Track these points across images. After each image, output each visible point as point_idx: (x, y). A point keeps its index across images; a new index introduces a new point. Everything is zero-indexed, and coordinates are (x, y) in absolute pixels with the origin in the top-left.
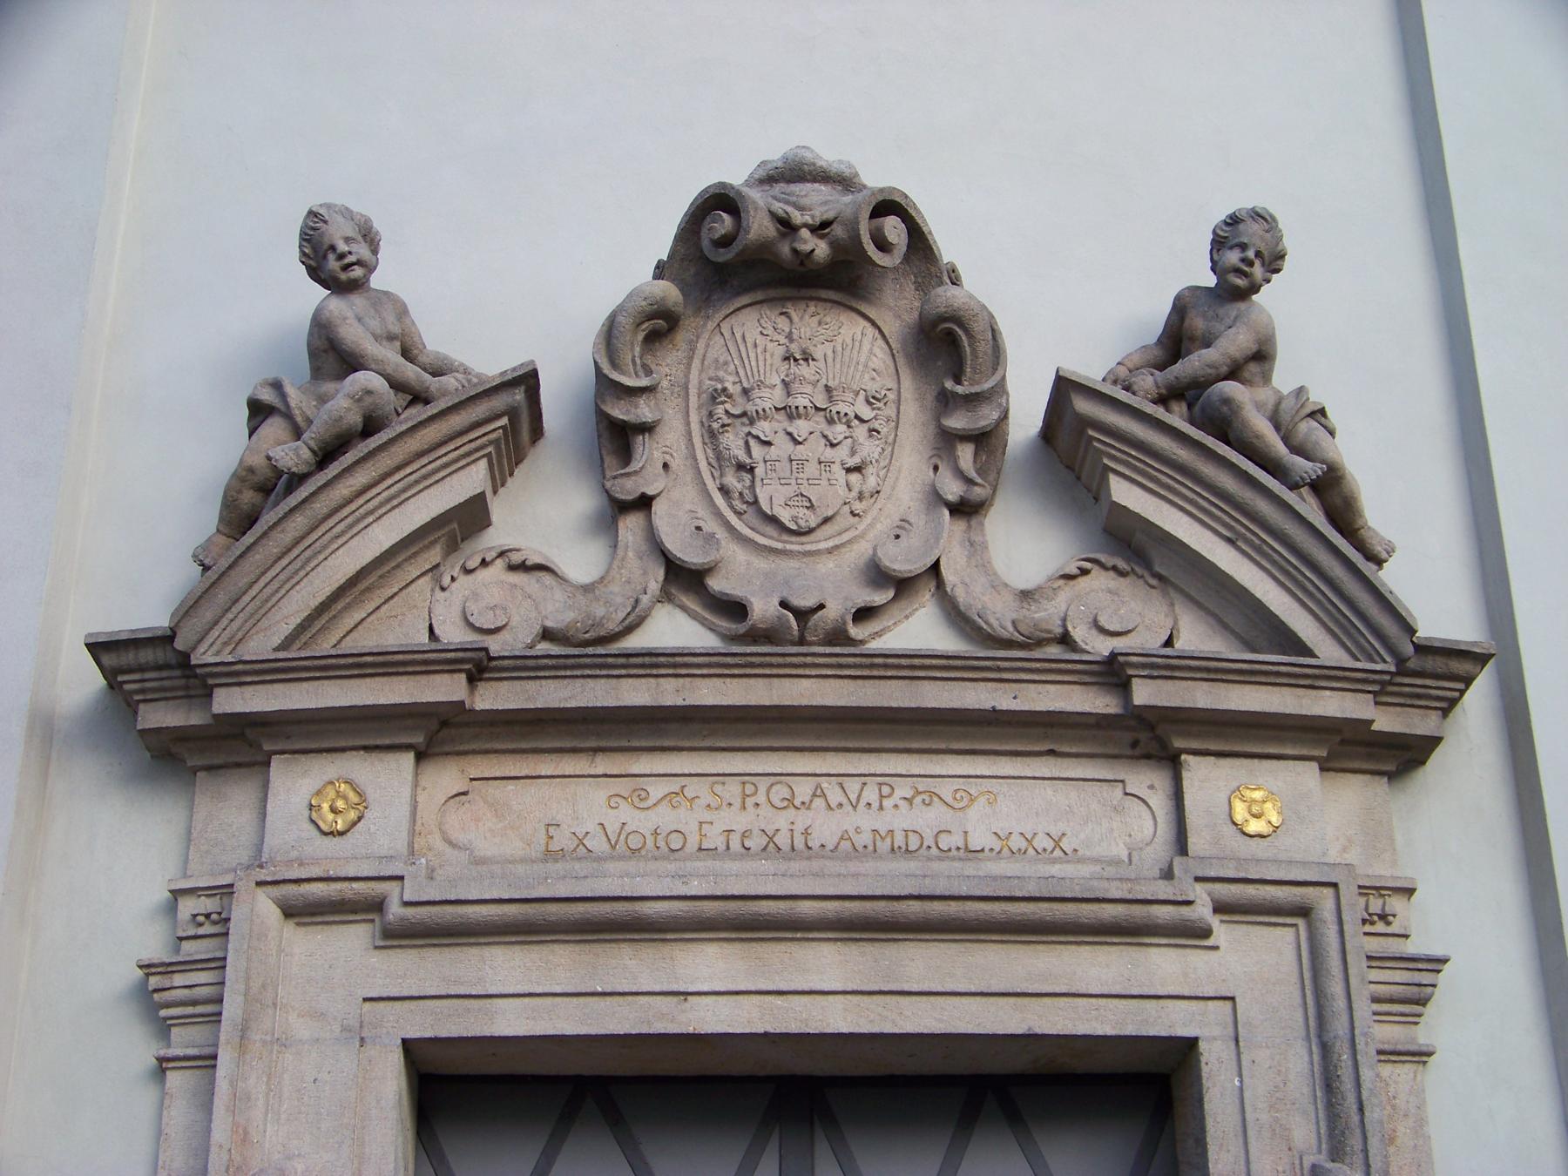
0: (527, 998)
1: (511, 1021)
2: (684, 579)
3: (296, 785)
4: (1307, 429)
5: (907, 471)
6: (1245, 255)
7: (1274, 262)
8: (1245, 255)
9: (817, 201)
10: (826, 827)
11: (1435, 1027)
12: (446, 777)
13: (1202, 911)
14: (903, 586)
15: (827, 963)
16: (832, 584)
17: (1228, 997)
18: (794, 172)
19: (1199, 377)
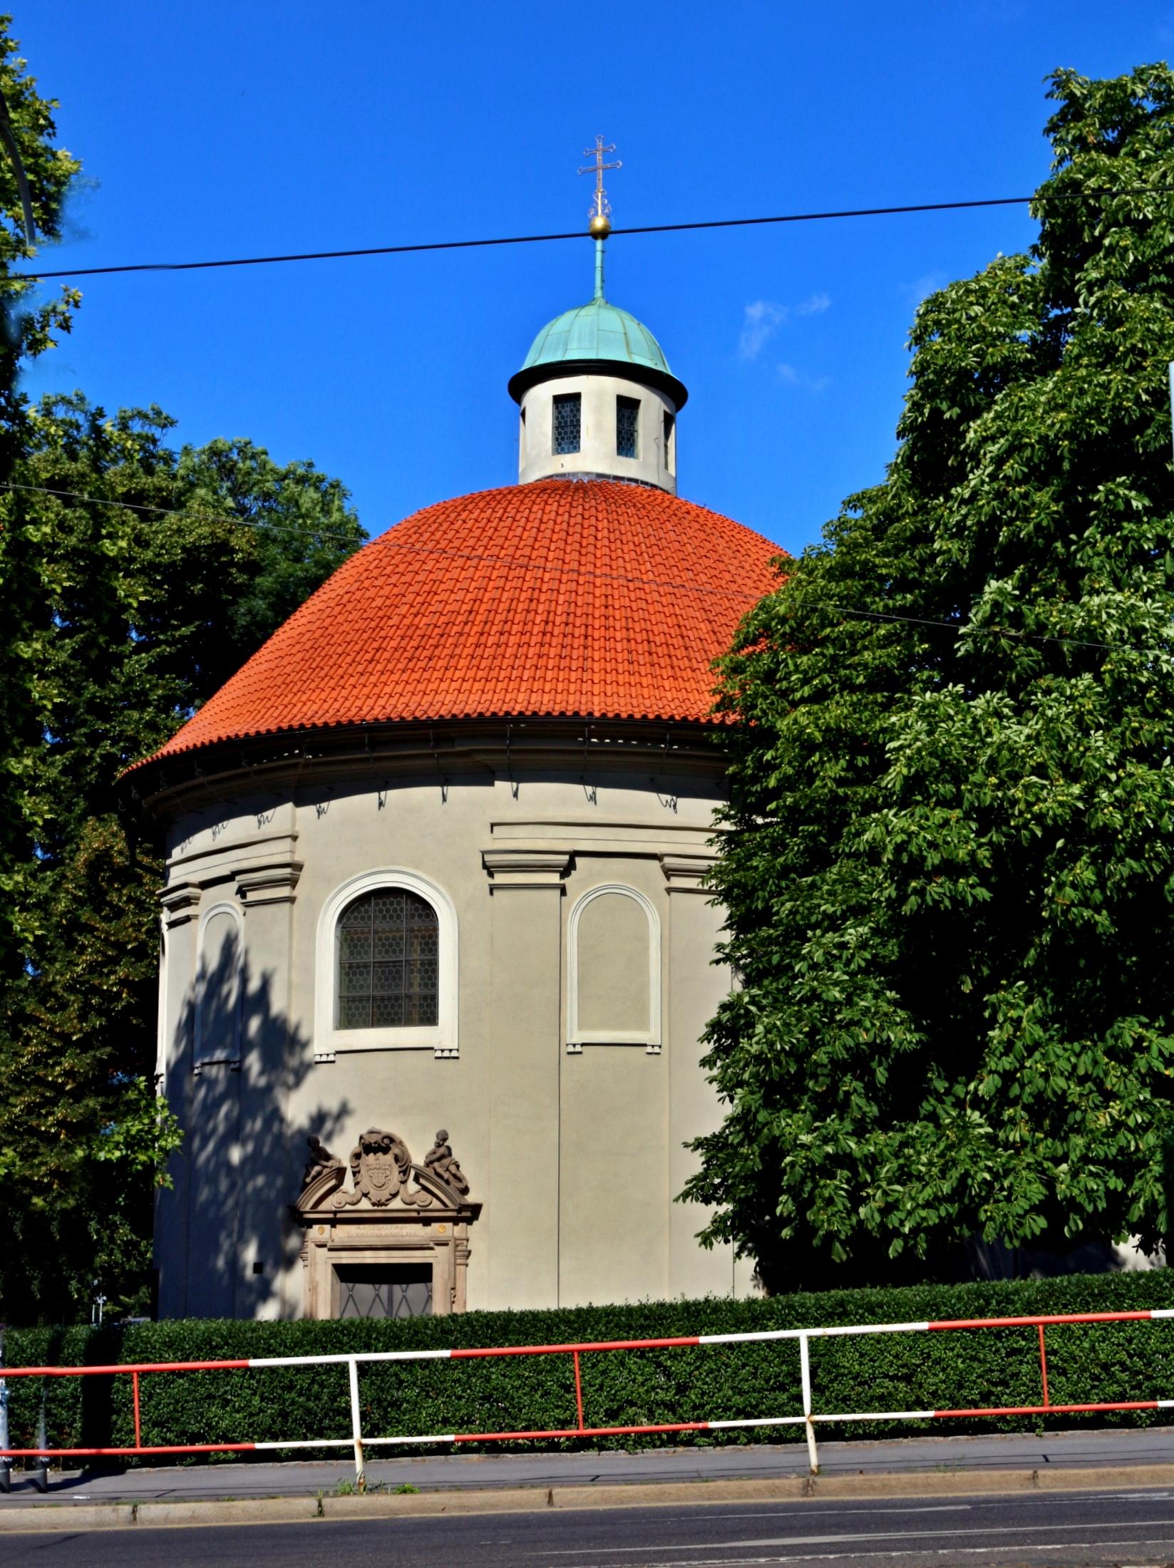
0: (347, 1258)
1: (344, 1261)
2: (365, 1195)
3: (316, 1227)
4: (453, 1168)
5: (396, 1176)
6: (443, 1138)
7: (445, 1140)
8: (443, 1138)
9: (373, 1139)
10: (383, 1232)
11: (470, 1261)
12: (333, 1226)
13: (432, 1245)
14: (394, 1196)
15: (383, 1253)
16: (384, 1195)
17: (439, 1259)
18: (371, 1132)
19: (442, 1151)
